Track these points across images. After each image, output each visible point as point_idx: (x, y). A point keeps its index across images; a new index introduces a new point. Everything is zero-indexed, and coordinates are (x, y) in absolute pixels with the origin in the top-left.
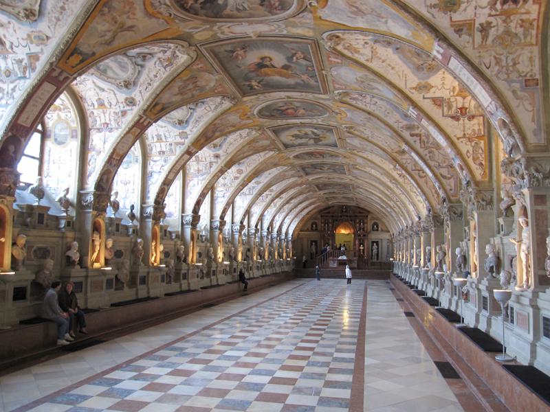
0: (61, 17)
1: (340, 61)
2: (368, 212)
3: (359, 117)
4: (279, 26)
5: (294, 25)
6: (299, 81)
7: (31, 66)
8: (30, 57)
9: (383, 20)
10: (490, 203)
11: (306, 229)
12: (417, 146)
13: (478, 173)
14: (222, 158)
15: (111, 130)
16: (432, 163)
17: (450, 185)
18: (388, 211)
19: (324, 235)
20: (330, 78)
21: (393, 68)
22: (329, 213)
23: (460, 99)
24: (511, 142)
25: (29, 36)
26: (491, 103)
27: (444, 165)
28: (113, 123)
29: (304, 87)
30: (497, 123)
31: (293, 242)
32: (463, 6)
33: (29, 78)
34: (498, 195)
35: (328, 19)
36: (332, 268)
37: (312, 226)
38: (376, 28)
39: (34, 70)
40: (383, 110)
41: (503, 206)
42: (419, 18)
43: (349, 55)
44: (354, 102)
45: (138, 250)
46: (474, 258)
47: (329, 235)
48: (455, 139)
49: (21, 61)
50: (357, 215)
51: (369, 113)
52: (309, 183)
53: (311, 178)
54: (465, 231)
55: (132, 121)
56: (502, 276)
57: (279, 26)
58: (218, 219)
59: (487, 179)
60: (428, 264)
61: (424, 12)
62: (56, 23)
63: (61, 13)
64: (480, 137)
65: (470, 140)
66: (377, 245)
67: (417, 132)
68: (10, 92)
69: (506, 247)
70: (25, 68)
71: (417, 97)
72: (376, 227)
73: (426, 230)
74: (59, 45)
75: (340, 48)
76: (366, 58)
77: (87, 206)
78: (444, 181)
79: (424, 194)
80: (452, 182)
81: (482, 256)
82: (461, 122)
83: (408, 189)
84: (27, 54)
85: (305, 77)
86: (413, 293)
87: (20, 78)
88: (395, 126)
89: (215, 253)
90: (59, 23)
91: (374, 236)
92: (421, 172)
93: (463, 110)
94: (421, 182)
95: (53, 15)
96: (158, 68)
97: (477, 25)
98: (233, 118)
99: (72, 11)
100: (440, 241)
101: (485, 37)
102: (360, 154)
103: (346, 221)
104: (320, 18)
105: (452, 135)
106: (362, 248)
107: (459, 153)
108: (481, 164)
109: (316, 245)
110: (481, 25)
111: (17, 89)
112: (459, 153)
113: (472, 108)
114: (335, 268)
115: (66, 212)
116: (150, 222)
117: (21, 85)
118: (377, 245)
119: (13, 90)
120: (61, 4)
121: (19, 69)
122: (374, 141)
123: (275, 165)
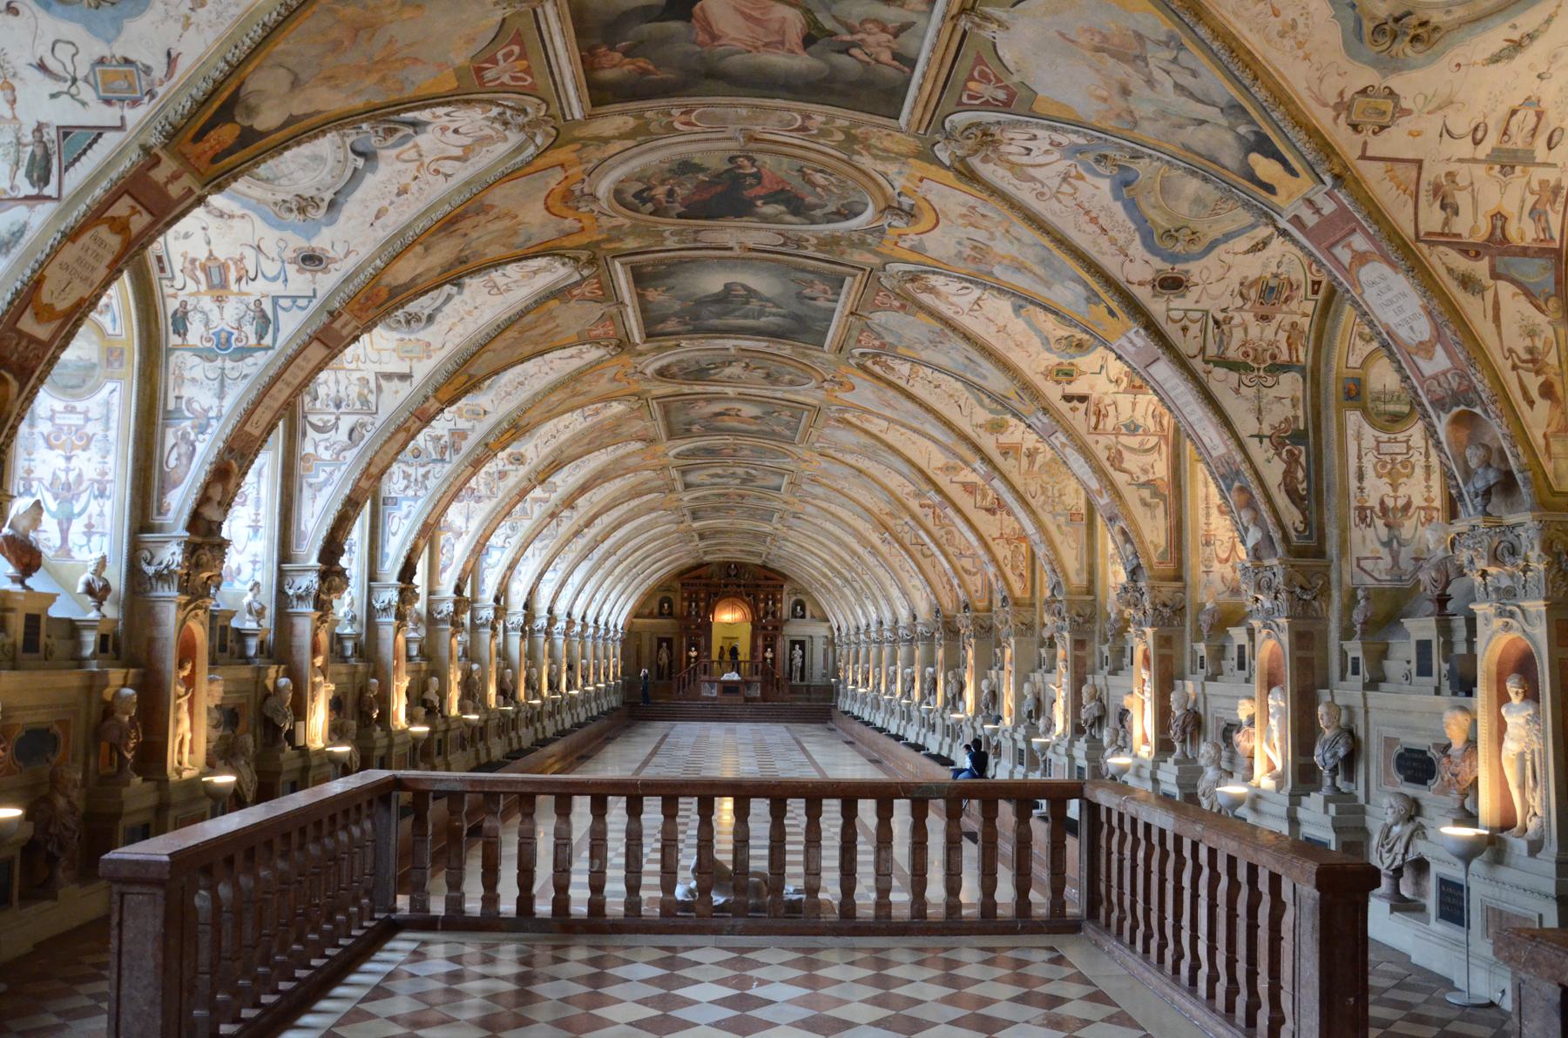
2: (785, 577)
3: (837, 469)
5: (797, 393)
11: (647, 611)
12: (929, 522)
14: (582, 510)
15: (479, 499)
16: (950, 550)
18: (833, 583)
19: (687, 628)
20: (815, 433)
22: (699, 577)
28: (482, 487)
29: (772, 435)
31: (624, 641)
34: (1041, 617)
36: (707, 698)
37: (661, 606)
39: (457, 451)
41: (1046, 634)
42: (964, 437)
43: (858, 423)
44: (839, 456)
45: (475, 684)
46: (1008, 701)
47: (698, 627)
48: (989, 541)
49: (439, 438)
50: (759, 584)
52: (688, 531)
53: (696, 525)
55: (515, 486)
56: (1042, 723)
58: (544, 613)
59: (1028, 595)
60: (931, 699)
61: (969, 430)
65: (1008, 542)
66: (802, 648)
71: (942, 480)
72: (799, 609)
73: (929, 639)
74: (499, 423)
75: (848, 416)
77: (443, 621)
78: (966, 577)
79: (930, 584)
80: (978, 580)
81: (1019, 698)
83: (897, 566)
85: (777, 429)
86: (904, 749)
87: (435, 461)
88: (898, 492)
89: (540, 679)
91: (795, 629)
94: (926, 563)
98: (631, 462)
100: (954, 664)
102: (817, 502)
103: (737, 595)
106: (769, 655)
107: (994, 560)
109: (670, 648)
112: (994, 560)
114: (714, 699)
115: (415, 630)
116: (486, 633)
118: (802, 648)
119: (425, 476)
123: (653, 510)
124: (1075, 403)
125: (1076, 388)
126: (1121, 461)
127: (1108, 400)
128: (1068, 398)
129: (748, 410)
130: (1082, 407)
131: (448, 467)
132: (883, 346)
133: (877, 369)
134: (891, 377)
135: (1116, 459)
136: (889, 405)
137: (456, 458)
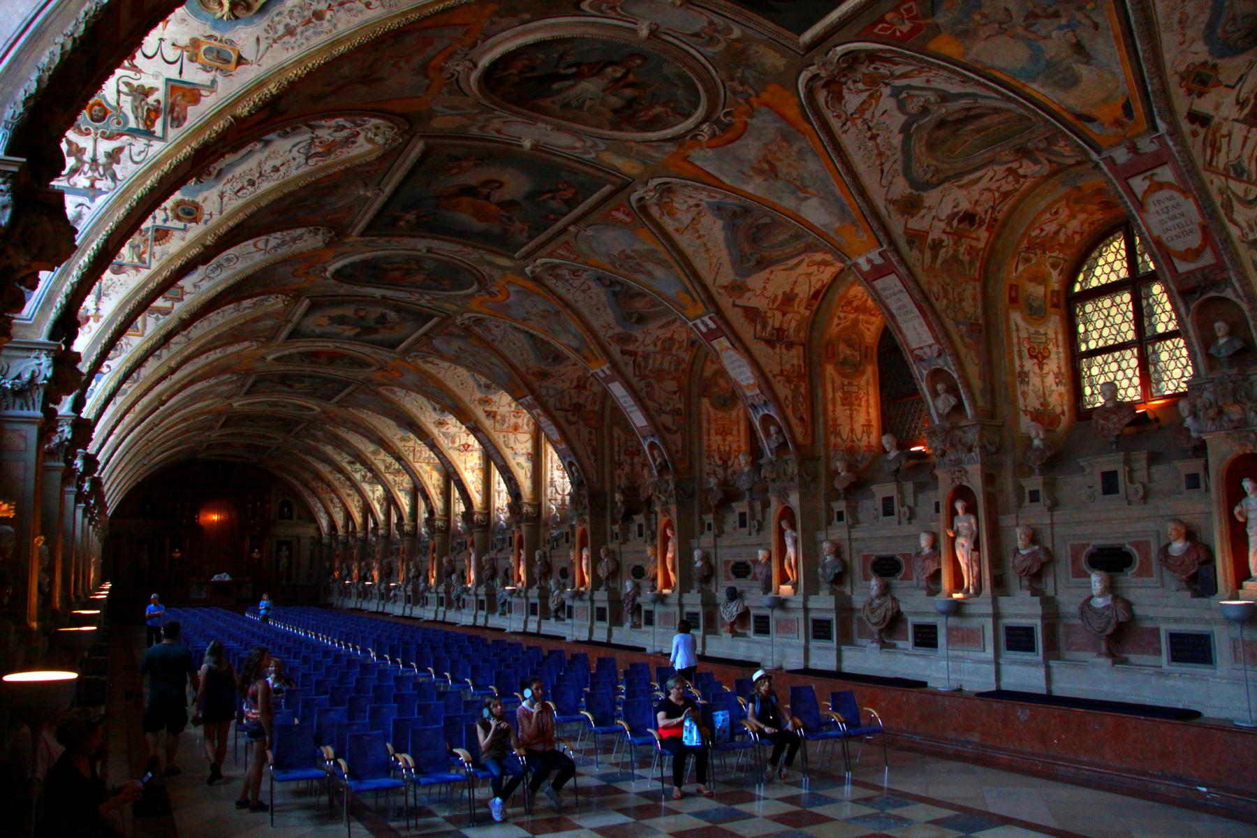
0: (299, 30)
1: (628, 220)
4: (595, 145)
6: (496, 229)
7: (172, 111)
8: (173, 88)
9: (802, 195)
10: (815, 478)
12: (629, 371)
13: (798, 431)
16: (650, 404)
17: (676, 445)
21: (707, 250)
23: (778, 315)
24: (953, 401)
25: (195, 43)
26: (930, 346)
27: (668, 409)
30: (925, 372)
32: (923, 211)
33: (163, 139)
35: (698, 163)
38: (775, 200)
39: (178, 121)
40: (594, 302)
41: (839, 485)
48: (770, 376)
49: (145, 93)
51: (567, 305)
54: (702, 522)
57: (595, 145)
62: (280, 38)
63: (309, 21)
64: (800, 377)
65: (789, 380)
67: (631, 347)
68: (102, 159)
69: (854, 544)
70: (153, 113)
71: (725, 302)
74: (260, 84)
76: (677, 225)
78: (667, 435)
80: (678, 438)
82: (777, 350)
84: (168, 80)
87: (133, 133)
90: (287, 39)
92: (569, 414)
93: (780, 330)
94: (571, 431)
95: (288, 20)
96: (295, 153)
97: (929, 240)
99: (335, 26)
101: (934, 257)
104: (686, 159)
105: (766, 370)
107: (775, 398)
108: (802, 419)
110: (933, 240)
111: (124, 156)
113: (791, 331)
117: (135, 150)
119: (114, 156)
120: (322, 6)
121: (135, 109)
122: (500, 347)
124: (1196, 127)
125: (1204, 105)
126: (1232, 211)
127: (1224, 131)
128: (1193, 117)
129: (515, 184)
130: (1202, 132)
131: (157, 147)
132: (915, 30)
133: (822, 96)
134: (829, 114)
135: (1229, 208)
136: (769, 170)
137: (173, 133)
